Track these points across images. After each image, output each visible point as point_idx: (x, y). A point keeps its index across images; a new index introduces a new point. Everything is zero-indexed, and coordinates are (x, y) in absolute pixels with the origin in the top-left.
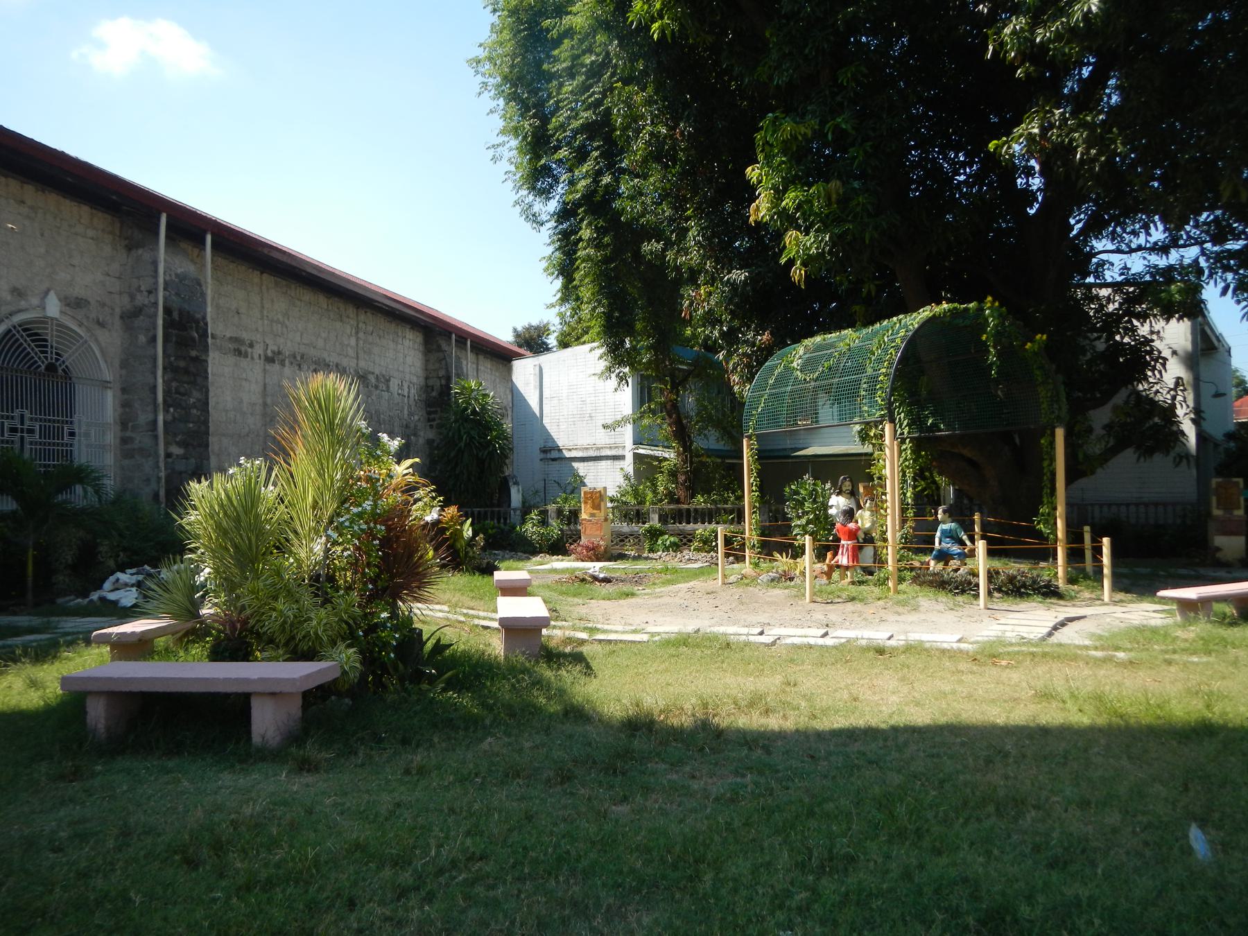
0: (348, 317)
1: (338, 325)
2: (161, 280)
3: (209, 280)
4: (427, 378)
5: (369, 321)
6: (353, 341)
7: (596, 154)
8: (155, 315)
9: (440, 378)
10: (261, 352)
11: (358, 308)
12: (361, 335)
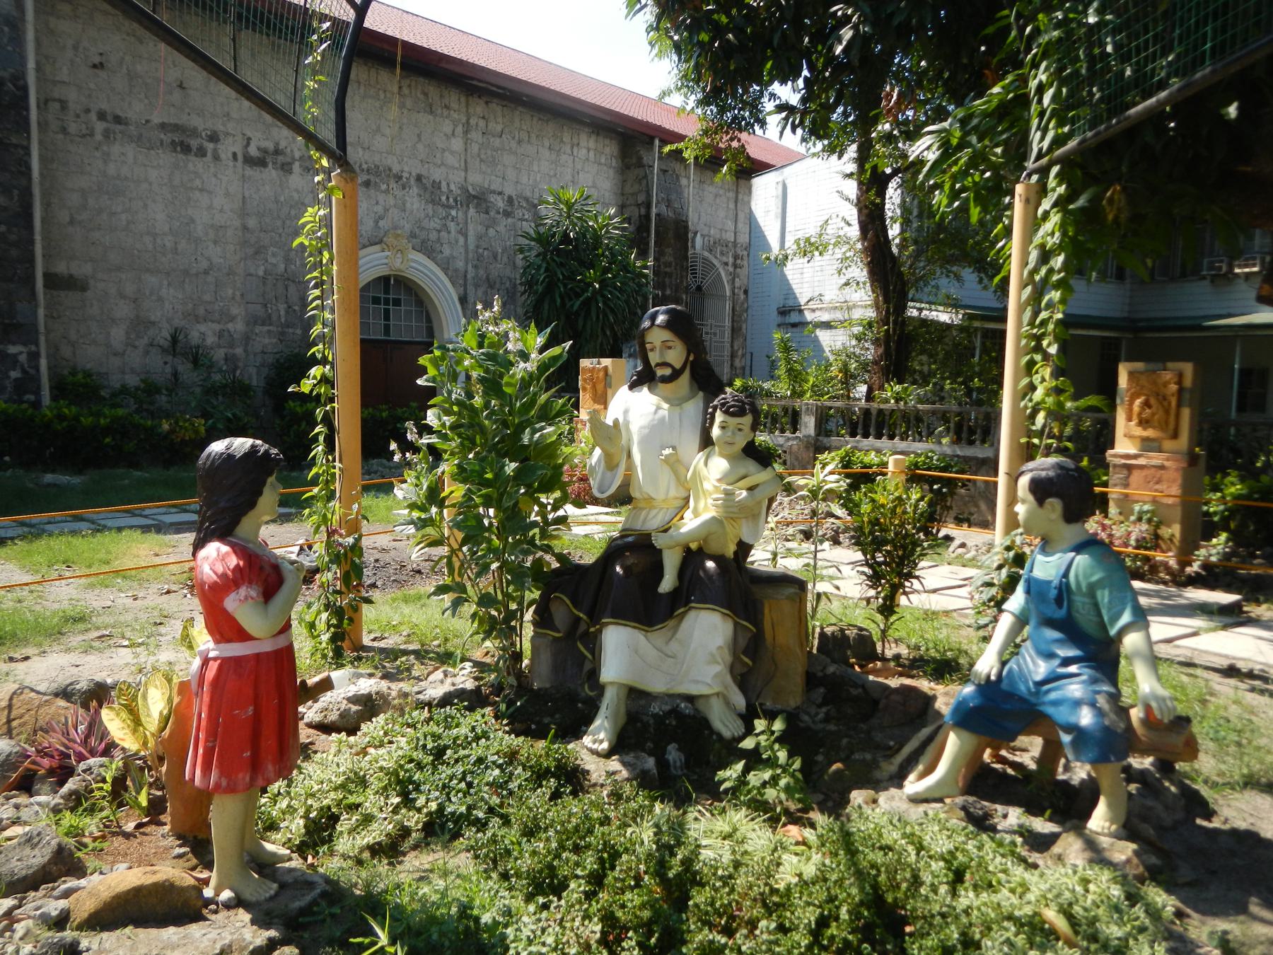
0: (447, 107)
1: (424, 118)
5: (498, 118)
6: (457, 144)
9: (638, 205)
10: (238, 149)
11: (467, 96)
12: (475, 135)
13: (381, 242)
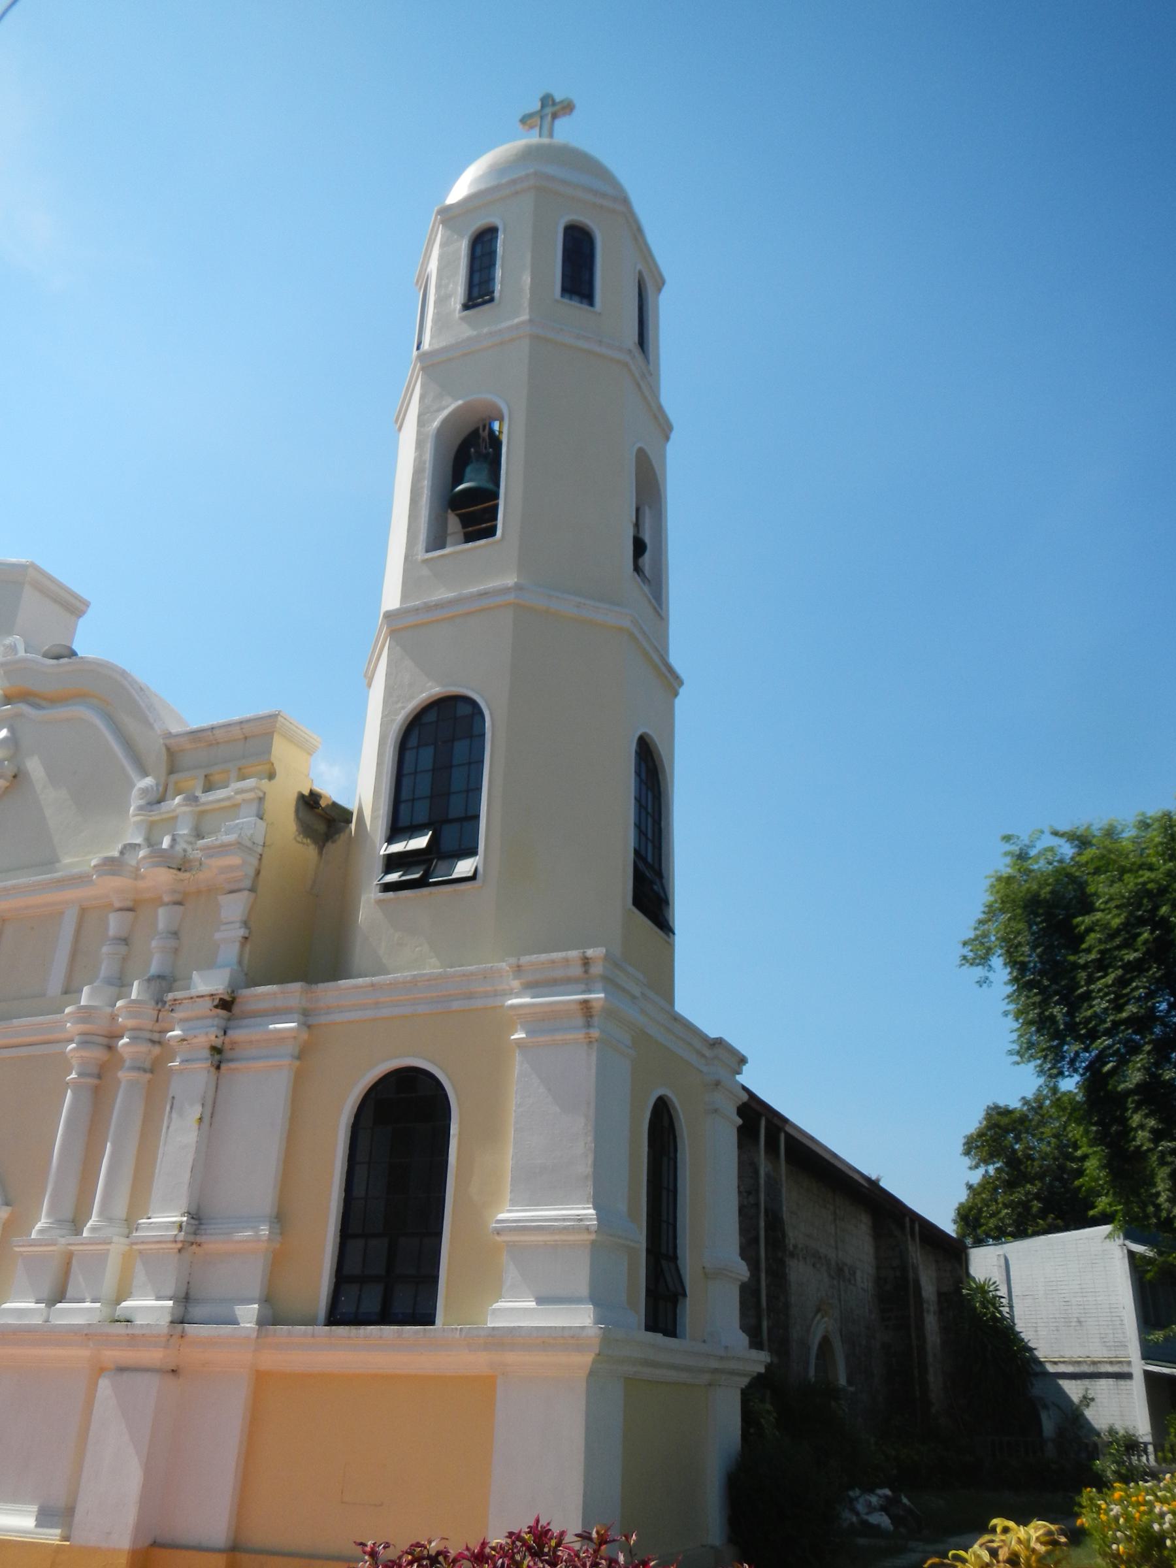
2: (762, 1181)
3: (784, 1178)
4: (878, 1268)
7: (1148, 1048)
8: (758, 1213)
13: (818, 1310)
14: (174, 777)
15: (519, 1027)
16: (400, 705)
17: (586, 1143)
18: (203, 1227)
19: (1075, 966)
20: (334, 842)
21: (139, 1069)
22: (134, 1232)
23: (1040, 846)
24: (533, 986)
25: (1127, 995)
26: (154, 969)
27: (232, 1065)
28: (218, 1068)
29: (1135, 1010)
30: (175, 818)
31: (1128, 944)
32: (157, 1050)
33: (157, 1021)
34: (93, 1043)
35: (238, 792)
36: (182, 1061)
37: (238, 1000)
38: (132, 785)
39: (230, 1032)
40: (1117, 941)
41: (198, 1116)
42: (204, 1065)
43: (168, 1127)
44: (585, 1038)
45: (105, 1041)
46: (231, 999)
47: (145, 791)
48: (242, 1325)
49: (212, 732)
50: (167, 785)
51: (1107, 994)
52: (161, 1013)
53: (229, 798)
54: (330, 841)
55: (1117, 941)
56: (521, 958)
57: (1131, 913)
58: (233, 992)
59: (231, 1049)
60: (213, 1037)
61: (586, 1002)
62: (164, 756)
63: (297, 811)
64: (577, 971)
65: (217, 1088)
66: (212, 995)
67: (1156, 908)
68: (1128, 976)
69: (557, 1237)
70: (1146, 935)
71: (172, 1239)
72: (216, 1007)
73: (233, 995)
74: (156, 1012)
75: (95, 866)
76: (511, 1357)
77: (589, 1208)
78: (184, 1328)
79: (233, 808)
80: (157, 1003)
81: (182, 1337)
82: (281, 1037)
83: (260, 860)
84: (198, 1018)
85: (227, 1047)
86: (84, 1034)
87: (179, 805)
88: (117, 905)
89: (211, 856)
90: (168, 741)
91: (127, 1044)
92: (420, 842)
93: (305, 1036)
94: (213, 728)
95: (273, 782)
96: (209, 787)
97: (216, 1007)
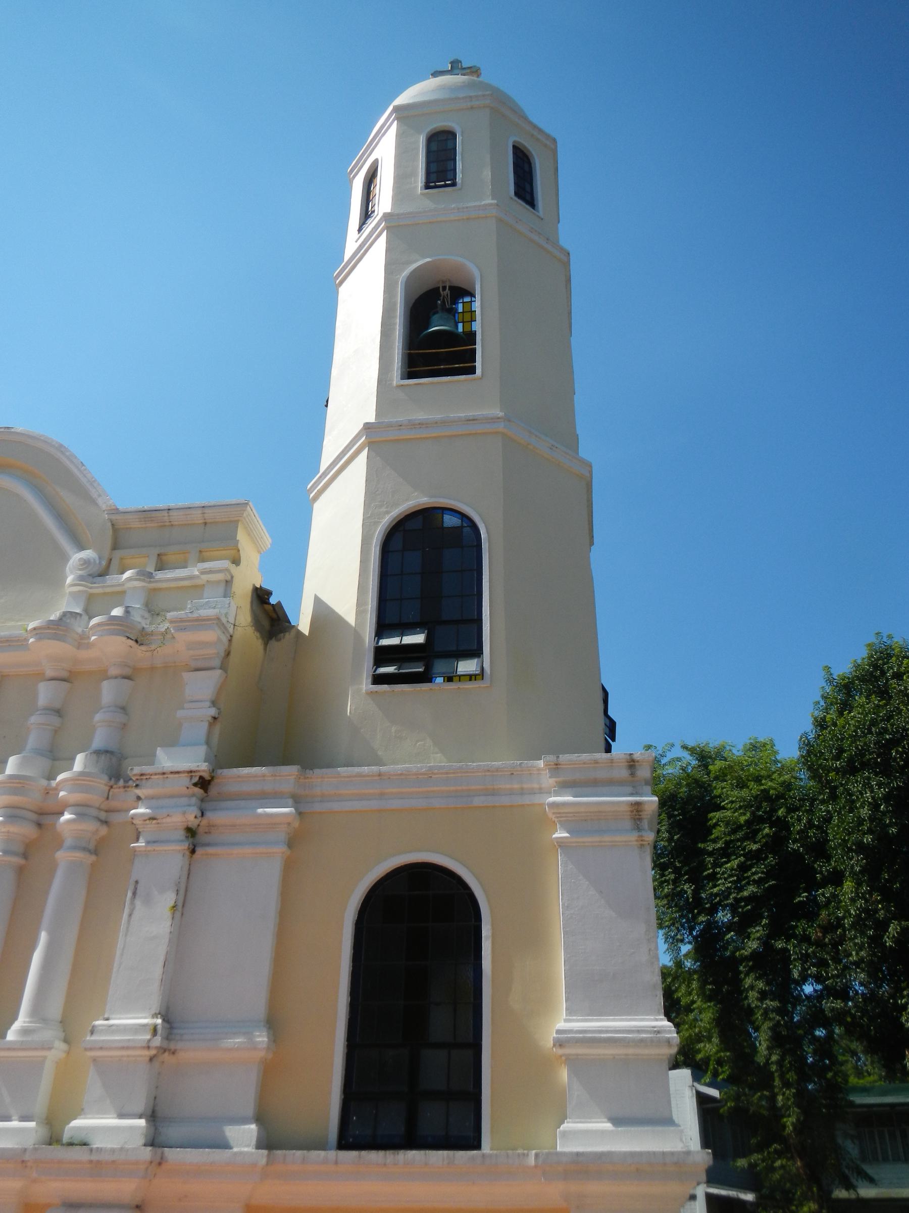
14: (118, 554)
15: (558, 826)
16: (383, 509)
17: (650, 950)
18: (176, 1031)
19: (704, 852)
20: (279, 640)
21: (85, 849)
22: (89, 1034)
23: (670, 756)
24: (566, 786)
25: (748, 877)
26: (98, 742)
27: (210, 850)
28: (193, 852)
29: (755, 890)
30: (123, 593)
31: (752, 836)
32: (104, 830)
33: (108, 798)
34: (24, 818)
35: (203, 572)
36: (148, 842)
37: (215, 781)
38: (65, 558)
39: (209, 814)
40: (740, 835)
41: (172, 903)
42: (178, 848)
43: (130, 915)
44: (637, 841)
45: (34, 817)
46: (210, 779)
47: (86, 563)
48: (235, 1150)
49: (168, 513)
50: (111, 560)
51: (731, 876)
52: (112, 790)
53: (191, 578)
54: (274, 638)
55: (740, 835)
56: (561, 756)
57: (753, 813)
58: (213, 771)
59: (206, 833)
60: (191, 818)
61: (638, 804)
62: (110, 532)
63: (252, 603)
64: (624, 773)
65: (189, 874)
66: (191, 772)
67: (774, 810)
68: (749, 863)
69: (631, 1051)
70: (767, 831)
71: (144, 1044)
72: (195, 785)
73: (213, 774)
74: (107, 788)
75: (35, 629)
76: (594, 1188)
77: (661, 1020)
78: (163, 1153)
79: (197, 589)
80: (110, 779)
81: (160, 1164)
82: (272, 823)
83: (230, 641)
84: (171, 796)
85: (201, 830)
86: (13, 807)
87: (129, 579)
88: (49, 673)
89: (184, 629)
90: (113, 517)
91: (69, 821)
92: (418, 639)
93: (296, 824)
94: (169, 510)
95: (238, 567)
96: (160, 567)
97: (195, 785)
